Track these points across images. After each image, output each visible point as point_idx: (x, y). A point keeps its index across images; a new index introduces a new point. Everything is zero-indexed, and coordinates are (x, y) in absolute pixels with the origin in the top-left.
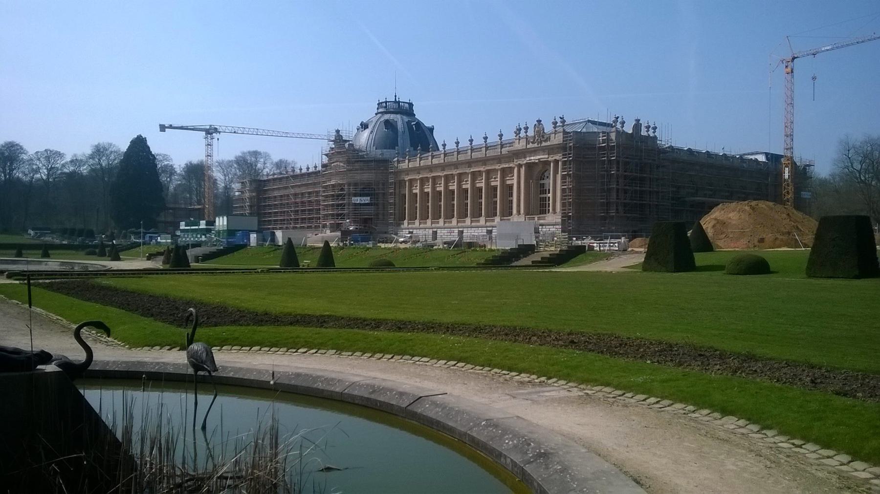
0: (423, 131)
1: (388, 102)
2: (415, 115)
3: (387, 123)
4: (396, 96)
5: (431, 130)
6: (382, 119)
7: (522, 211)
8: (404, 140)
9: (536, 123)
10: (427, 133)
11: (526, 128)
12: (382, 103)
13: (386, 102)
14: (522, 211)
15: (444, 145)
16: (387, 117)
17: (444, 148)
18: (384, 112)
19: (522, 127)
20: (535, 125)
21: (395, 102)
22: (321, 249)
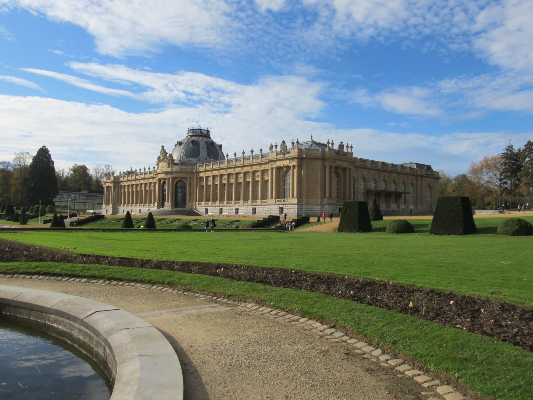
0: (215, 147)
1: (194, 129)
2: (211, 138)
3: (193, 142)
4: (199, 126)
5: (220, 146)
6: (190, 140)
7: (274, 196)
8: (203, 152)
9: (282, 143)
10: (218, 148)
11: (276, 146)
12: (191, 130)
13: (193, 130)
14: (274, 196)
15: (227, 156)
16: (194, 138)
17: (227, 158)
18: (192, 135)
19: (274, 145)
20: (281, 144)
21: (199, 129)
22: (122, 221)
